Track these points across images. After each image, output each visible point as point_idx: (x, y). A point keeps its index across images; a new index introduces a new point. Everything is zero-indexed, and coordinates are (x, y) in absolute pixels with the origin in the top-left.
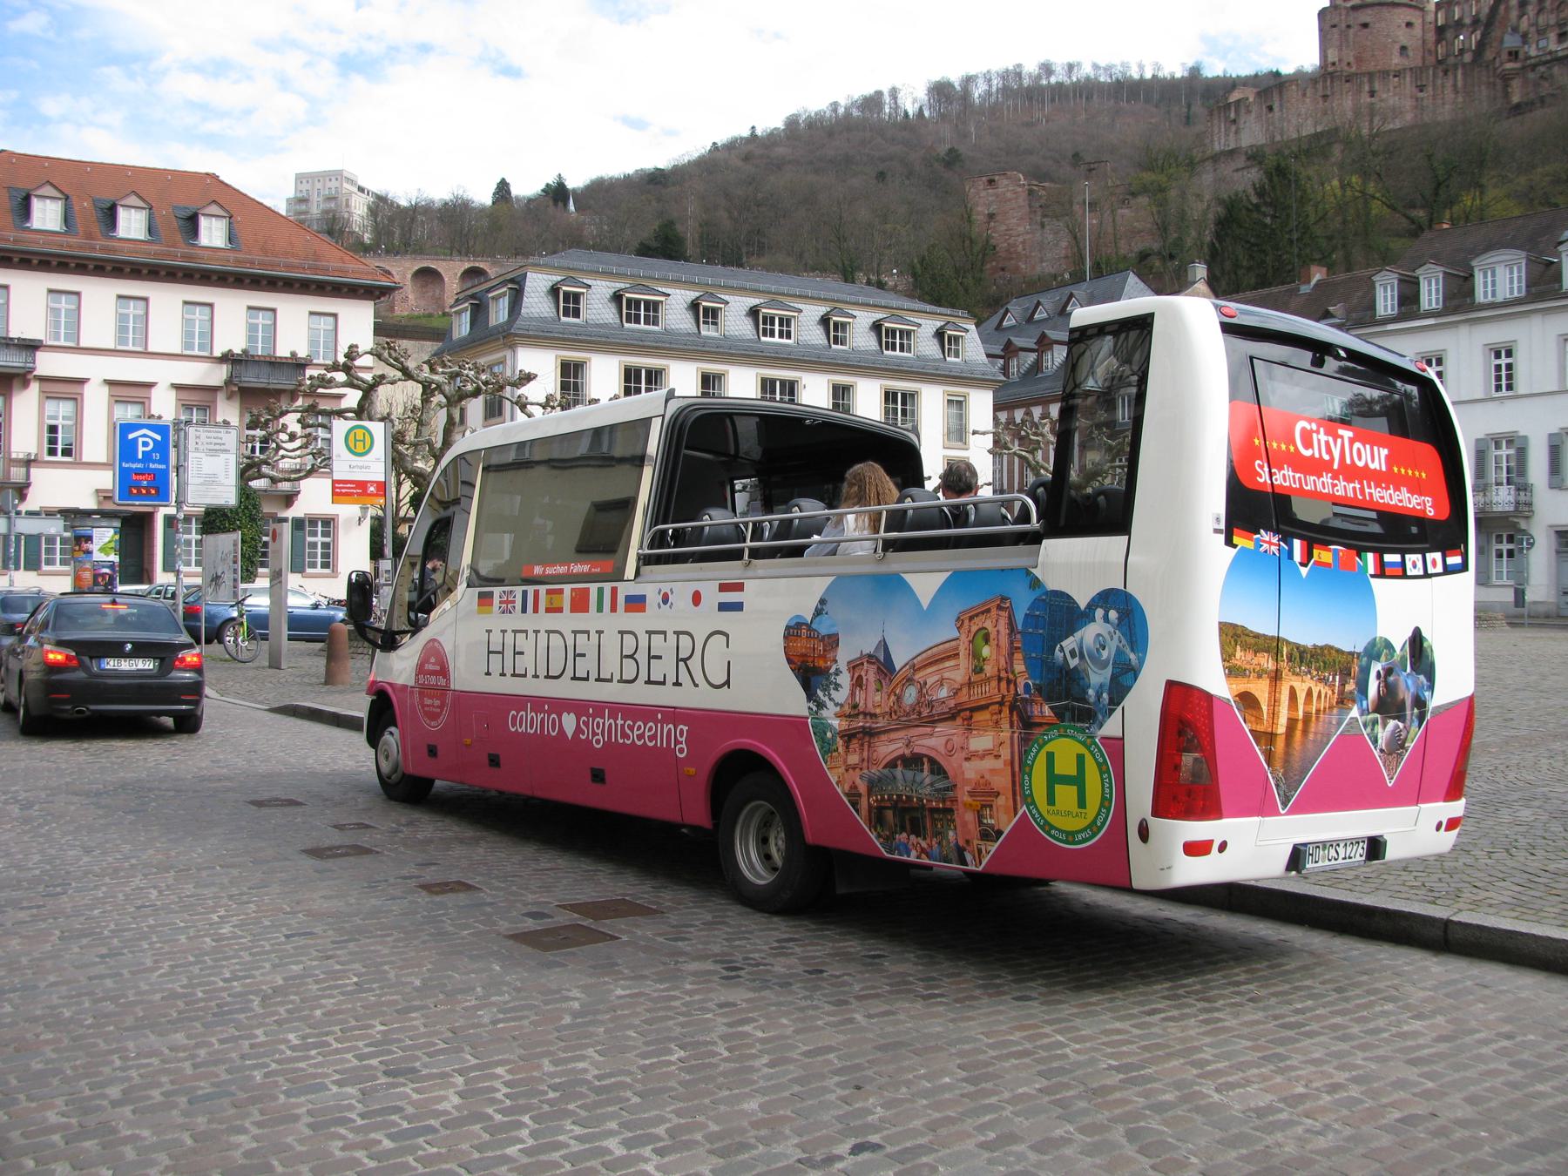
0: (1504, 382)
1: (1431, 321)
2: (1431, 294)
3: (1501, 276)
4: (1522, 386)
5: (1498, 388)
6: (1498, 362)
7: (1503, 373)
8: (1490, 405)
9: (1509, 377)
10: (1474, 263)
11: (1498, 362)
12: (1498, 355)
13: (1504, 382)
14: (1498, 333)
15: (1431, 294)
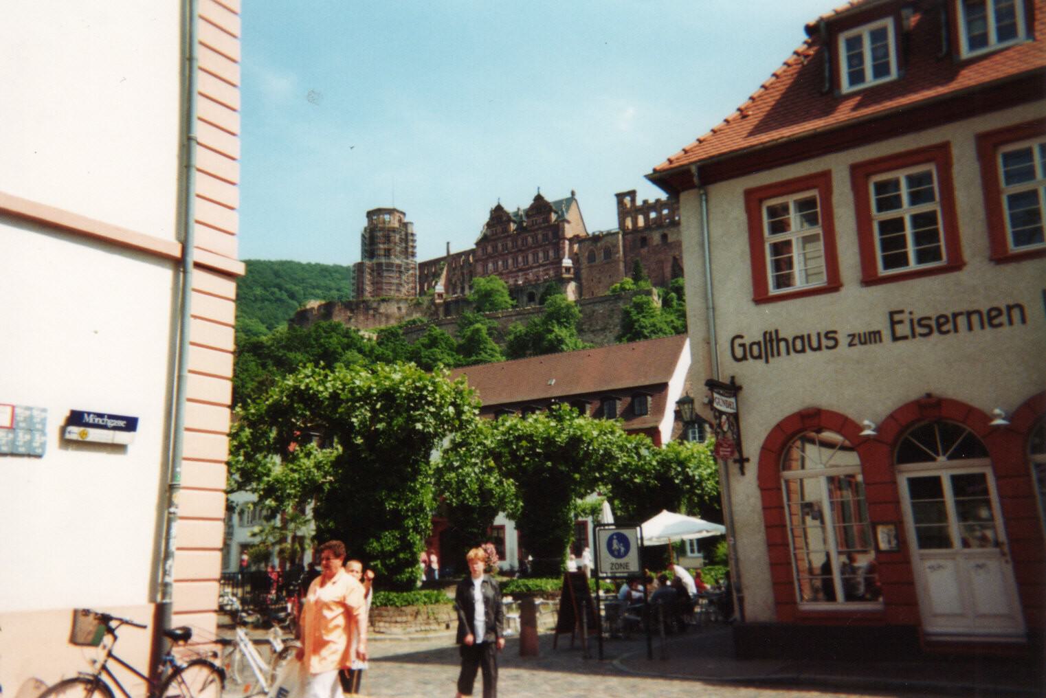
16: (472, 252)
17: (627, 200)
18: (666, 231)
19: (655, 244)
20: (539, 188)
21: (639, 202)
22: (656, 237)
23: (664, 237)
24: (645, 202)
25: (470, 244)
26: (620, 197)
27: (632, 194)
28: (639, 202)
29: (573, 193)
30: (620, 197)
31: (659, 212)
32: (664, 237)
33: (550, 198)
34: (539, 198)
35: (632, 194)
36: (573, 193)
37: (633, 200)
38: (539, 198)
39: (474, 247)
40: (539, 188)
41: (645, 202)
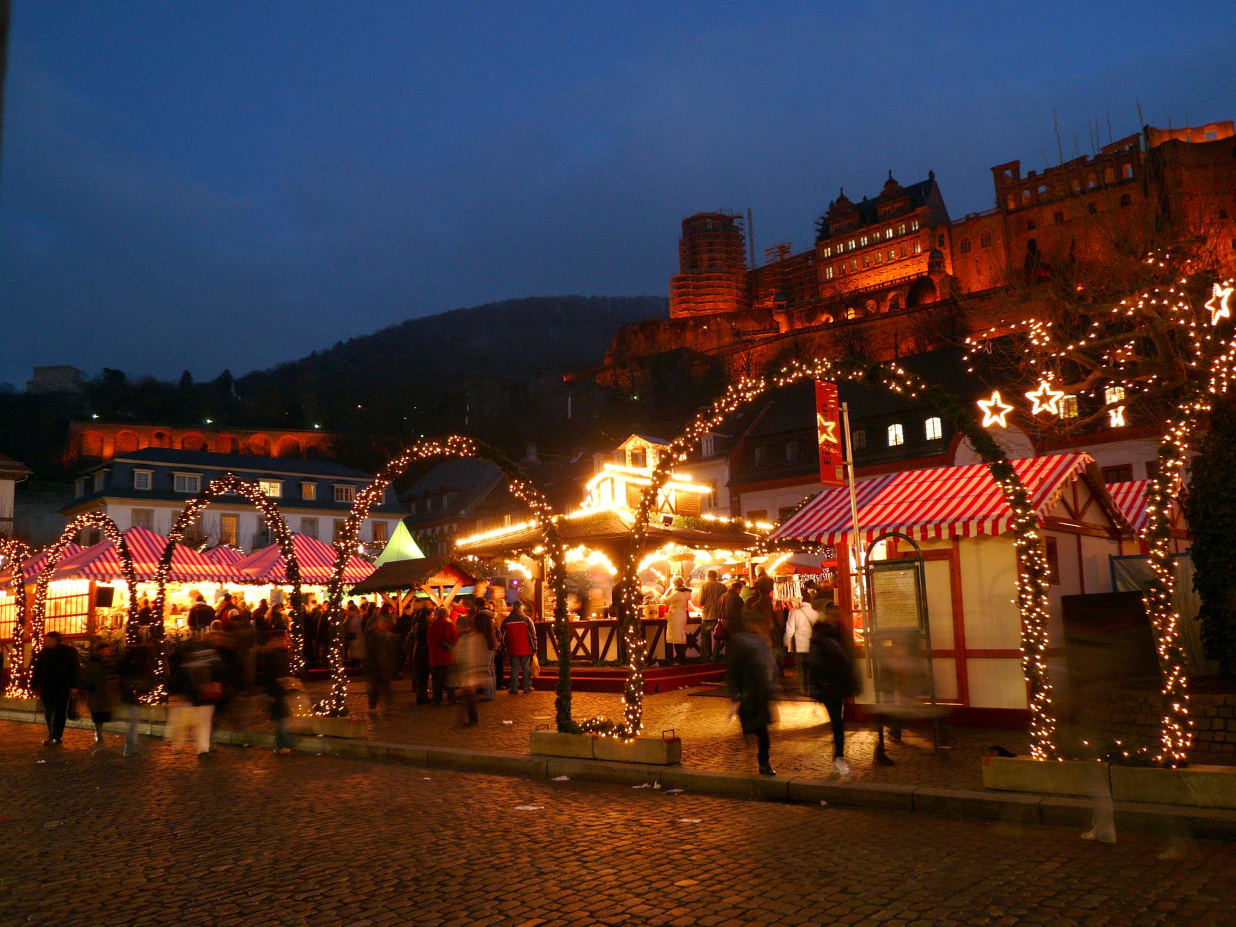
17: (1008, 173)
21: (1024, 175)
22: (1048, 214)
23: (1059, 216)
25: (877, 195)
26: (998, 171)
27: (1014, 166)
28: (1024, 175)
29: (931, 174)
30: (998, 171)
31: (1034, 189)
33: (905, 182)
34: (891, 183)
35: (1014, 166)
36: (931, 174)
38: (891, 183)
41: (1032, 174)
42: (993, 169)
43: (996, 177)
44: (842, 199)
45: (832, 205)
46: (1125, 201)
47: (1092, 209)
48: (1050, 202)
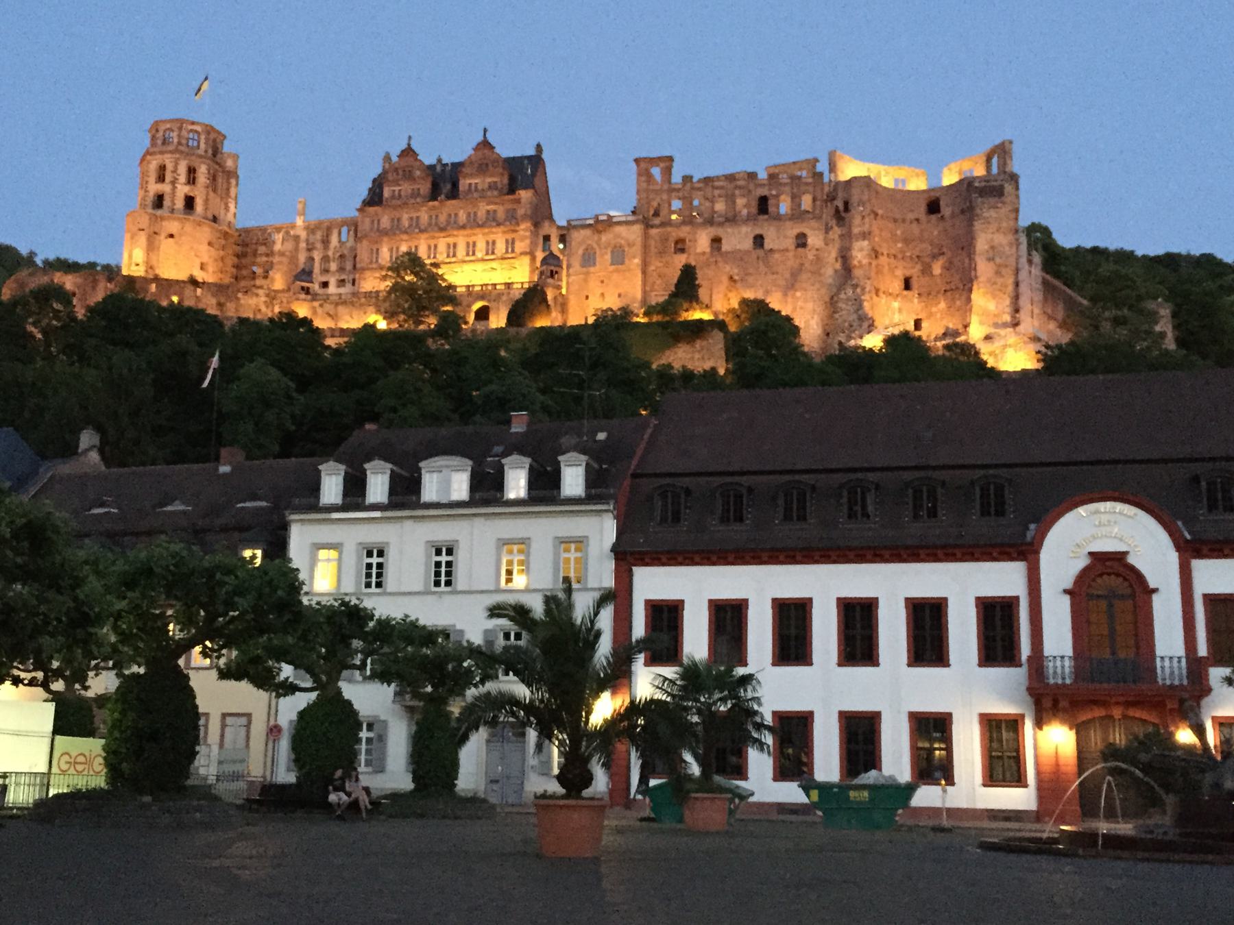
0: (443, 579)
1: (377, 514)
2: (378, 486)
3: (448, 480)
4: (461, 582)
5: (437, 584)
6: (438, 559)
7: (443, 569)
8: (430, 598)
9: (448, 574)
10: (422, 464)
11: (438, 559)
12: (438, 552)
13: (443, 579)
14: (442, 531)
15: (378, 486)
16: (354, 225)
17: (656, 172)
18: (720, 232)
19: (699, 250)
20: (485, 131)
21: (677, 178)
22: (702, 241)
23: (716, 241)
24: (687, 179)
27: (667, 162)
28: (677, 178)
29: (539, 148)
32: (716, 241)
34: (485, 144)
35: (667, 162)
36: (539, 148)
37: (668, 171)
38: (485, 144)
39: (357, 214)
40: (485, 131)
41: (687, 179)
42: (637, 161)
43: (639, 175)
44: (409, 152)
45: (387, 158)
46: (801, 241)
47: (759, 240)
48: (710, 222)
